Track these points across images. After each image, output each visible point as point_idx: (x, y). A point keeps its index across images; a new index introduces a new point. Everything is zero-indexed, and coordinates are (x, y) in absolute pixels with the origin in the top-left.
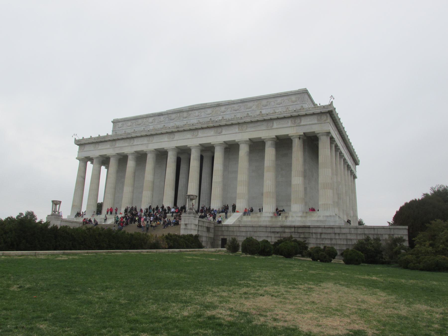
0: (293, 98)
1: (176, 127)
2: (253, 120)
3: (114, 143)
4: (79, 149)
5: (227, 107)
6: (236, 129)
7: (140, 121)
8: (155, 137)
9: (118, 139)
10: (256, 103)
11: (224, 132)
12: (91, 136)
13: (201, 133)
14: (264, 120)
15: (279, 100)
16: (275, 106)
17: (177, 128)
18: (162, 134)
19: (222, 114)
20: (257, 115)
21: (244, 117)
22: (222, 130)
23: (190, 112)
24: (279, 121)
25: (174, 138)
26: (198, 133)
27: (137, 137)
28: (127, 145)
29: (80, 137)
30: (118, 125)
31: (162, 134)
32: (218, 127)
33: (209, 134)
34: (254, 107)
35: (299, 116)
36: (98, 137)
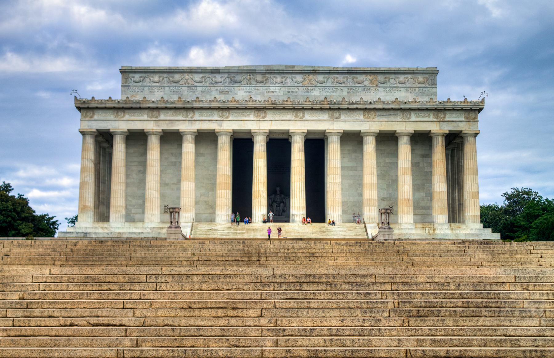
0: (421, 78)
2: (386, 107)
3: (155, 113)
4: (82, 115)
5: (327, 76)
6: (361, 116)
7: (177, 77)
8: (231, 111)
9: (166, 108)
10: (369, 77)
11: (343, 117)
12: (110, 98)
13: (308, 116)
14: (401, 109)
15: (402, 78)
16: (395, 85)
17: (272, 104)
18: (246, 109)
19: (319, 85)
20: (392, 102)
21: (375, 102)
22: (340, 115)
23: (268, 75)
24: (420, 112)
25: (265, 117)
26: (304, 114)
27: (202, 108)
28: (180, 118)
29: (86, 96)
30: (133, 77)
31: (246, 109)
32: (334, 109)
33: (321, 118)
34: (367, 83)
35: (445, 110)
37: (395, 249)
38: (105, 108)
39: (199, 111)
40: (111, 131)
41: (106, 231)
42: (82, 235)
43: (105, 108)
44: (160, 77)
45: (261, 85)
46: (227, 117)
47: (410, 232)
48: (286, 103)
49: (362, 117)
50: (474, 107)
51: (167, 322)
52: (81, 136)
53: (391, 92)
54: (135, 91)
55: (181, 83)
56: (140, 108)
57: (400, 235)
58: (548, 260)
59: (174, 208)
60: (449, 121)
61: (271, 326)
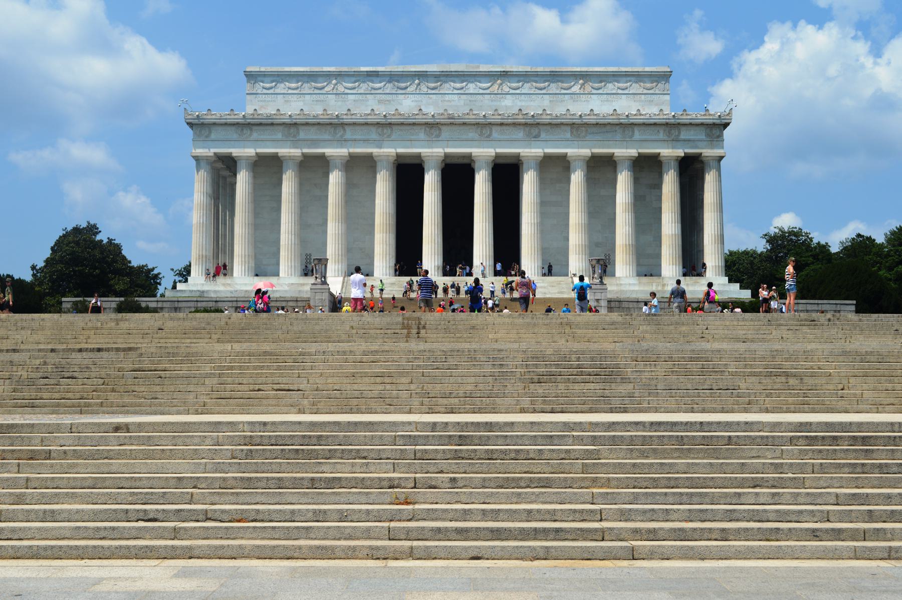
1: (446, 116)
3: (292, 130)
4: (195, 134)
8: (394, 128)
11: (543, 135)
16: (614, 92)
18: (414, 124)
19: (512, 91)
22: (539, 132)
25: (438, 136)
27: (354, 124)
28: (326, 137)
36: (253, 115)
37: (559, 321)
38: (226, 124)
39: (351, 127)
41: (229, 289)
42: (198, 294)
45: (433, 92)
46: (389, 136)
47: (632, 288)
48: (467, 117)
49: (568, 135)
50: (718, 122)
51: (335, 388)
52: (195, 162)
53: (607, 101)
54: (264, 101)
56: (272, 124)
57: (617, 292)
58: (713, 332)
59: (320, 260)
60: (684, 140)
61: (418, 391)
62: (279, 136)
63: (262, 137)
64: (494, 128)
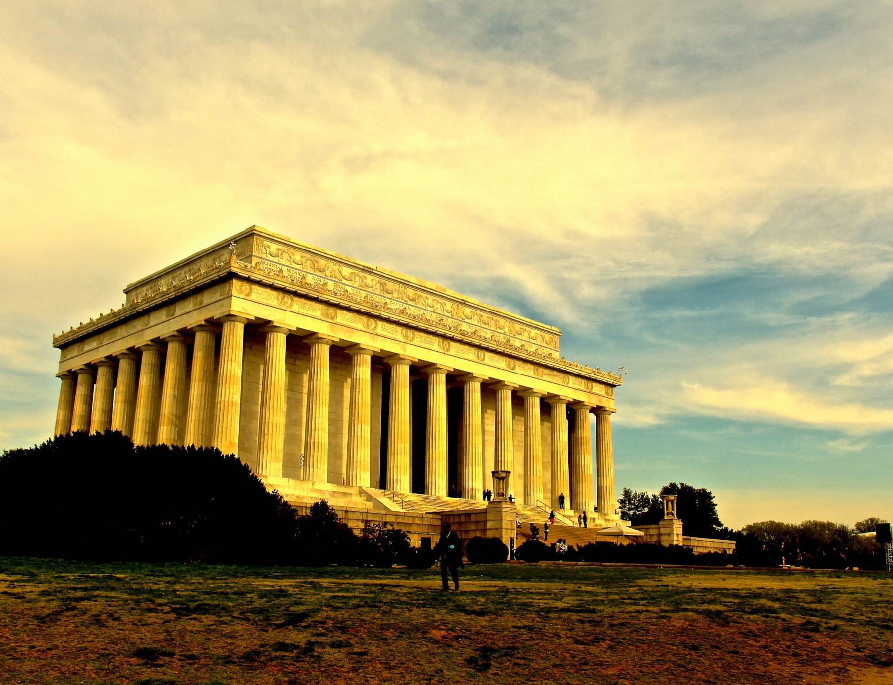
3: (332, 310)
6: (530, 370)
7: (322, 263)
11: (517, 370)
19: (467, 320)
25: (448, 350)
30: (269, 247)
33: (498, 365)
34: (506, 330)
40: (275, 324)
43: (272, 287)
44: (302, 257)
46: (412, 340)
55: (328, 273)
62: (318, 314)
63: (302, 311)
64: (488, 354)
